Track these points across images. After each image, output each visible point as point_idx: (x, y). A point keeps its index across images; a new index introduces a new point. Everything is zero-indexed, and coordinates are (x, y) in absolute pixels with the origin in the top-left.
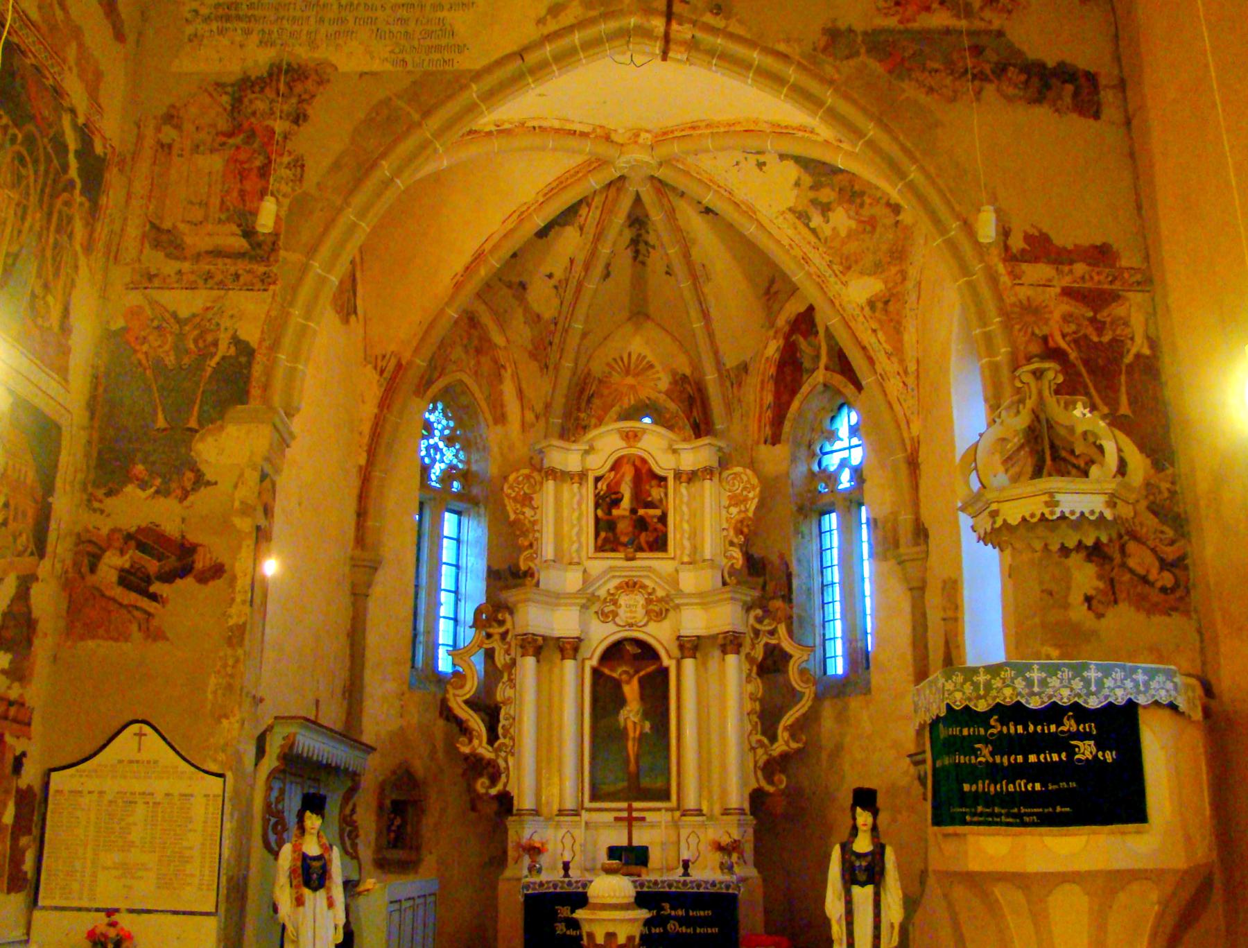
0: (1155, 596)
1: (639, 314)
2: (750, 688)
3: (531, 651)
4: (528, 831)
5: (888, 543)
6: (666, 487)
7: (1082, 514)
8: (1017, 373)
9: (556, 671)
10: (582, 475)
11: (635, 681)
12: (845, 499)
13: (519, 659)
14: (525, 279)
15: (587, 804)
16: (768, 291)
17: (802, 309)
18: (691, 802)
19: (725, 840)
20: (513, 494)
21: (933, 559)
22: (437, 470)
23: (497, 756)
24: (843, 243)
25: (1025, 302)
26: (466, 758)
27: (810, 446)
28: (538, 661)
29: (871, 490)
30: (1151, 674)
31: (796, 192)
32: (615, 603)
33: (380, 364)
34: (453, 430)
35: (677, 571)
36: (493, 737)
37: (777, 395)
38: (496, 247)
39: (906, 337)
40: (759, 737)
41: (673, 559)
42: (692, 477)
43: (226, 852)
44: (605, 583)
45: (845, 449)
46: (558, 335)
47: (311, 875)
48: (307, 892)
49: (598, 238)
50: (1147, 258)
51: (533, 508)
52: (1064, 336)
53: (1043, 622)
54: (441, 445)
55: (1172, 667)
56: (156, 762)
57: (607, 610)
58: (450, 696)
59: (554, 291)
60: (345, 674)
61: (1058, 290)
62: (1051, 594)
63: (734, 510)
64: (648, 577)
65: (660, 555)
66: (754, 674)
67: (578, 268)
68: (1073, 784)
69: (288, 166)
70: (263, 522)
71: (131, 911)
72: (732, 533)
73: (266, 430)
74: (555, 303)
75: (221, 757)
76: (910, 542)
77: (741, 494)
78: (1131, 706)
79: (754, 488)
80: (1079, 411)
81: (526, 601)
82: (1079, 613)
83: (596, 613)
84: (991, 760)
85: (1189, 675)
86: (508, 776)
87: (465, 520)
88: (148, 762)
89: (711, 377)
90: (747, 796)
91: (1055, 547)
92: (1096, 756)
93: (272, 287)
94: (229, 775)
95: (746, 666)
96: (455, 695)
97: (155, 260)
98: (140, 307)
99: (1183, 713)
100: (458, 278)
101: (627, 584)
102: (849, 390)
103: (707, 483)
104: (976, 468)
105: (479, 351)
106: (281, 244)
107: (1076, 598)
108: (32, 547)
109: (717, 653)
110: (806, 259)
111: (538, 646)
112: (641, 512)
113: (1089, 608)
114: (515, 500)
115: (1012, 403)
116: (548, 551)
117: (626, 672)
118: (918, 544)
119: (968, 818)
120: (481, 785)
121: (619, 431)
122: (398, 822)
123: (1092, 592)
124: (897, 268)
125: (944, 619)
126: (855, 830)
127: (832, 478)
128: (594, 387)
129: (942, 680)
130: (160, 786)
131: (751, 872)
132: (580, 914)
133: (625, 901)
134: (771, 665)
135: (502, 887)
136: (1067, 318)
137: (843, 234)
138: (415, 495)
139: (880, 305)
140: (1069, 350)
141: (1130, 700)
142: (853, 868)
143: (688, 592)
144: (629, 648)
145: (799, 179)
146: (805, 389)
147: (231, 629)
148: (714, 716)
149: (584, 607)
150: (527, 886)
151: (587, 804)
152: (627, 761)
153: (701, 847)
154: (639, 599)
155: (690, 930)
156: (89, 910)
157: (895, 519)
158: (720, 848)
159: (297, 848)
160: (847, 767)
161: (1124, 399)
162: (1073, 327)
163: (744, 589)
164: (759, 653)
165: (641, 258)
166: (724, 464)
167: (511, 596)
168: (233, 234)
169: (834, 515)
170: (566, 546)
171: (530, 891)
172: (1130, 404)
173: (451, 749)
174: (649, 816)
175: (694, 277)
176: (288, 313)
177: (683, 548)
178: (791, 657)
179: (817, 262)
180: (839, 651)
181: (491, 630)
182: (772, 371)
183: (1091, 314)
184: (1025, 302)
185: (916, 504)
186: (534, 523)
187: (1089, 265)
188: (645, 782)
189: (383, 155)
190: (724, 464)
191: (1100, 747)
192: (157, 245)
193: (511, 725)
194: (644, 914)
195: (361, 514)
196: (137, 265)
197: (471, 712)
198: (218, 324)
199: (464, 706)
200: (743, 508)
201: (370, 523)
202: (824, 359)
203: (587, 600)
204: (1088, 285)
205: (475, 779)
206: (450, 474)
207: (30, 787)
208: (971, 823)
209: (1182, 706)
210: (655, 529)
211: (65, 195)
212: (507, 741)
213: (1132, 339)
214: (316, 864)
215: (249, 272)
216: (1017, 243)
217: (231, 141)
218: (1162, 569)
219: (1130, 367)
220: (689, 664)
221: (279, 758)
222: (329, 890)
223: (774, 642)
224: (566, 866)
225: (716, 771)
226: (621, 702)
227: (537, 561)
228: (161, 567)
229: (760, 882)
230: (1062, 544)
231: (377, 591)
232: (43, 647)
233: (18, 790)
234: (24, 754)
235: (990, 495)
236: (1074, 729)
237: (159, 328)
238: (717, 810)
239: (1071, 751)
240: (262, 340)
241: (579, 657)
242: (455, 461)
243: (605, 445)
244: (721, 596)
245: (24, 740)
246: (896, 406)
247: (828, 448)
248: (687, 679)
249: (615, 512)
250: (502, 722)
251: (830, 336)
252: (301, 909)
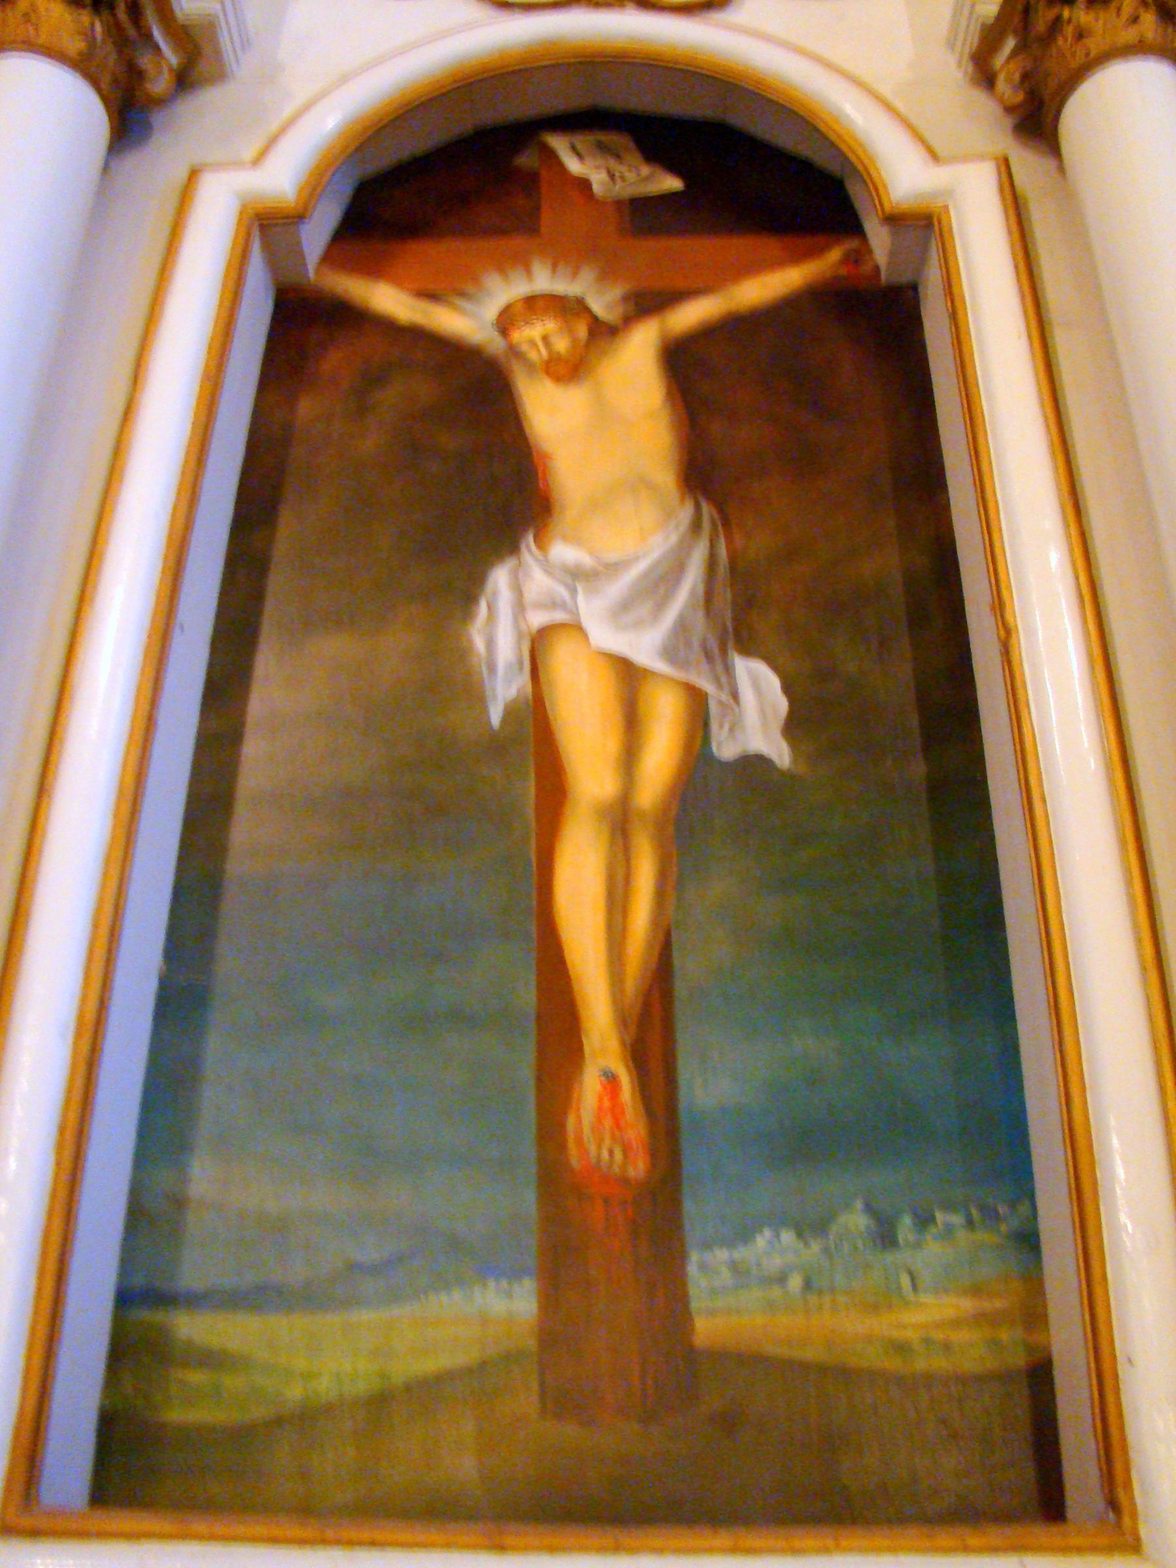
117: (534, 304)
188: (756, 1284)
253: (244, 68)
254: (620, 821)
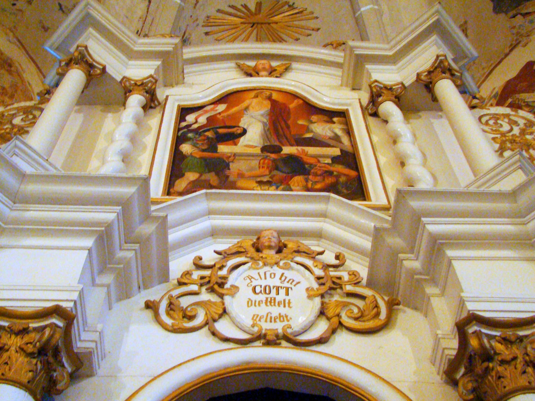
32: (217, 286)
83: (150, 306)
210: (330, 173)
249: (224, 149)
253: (102, 368)
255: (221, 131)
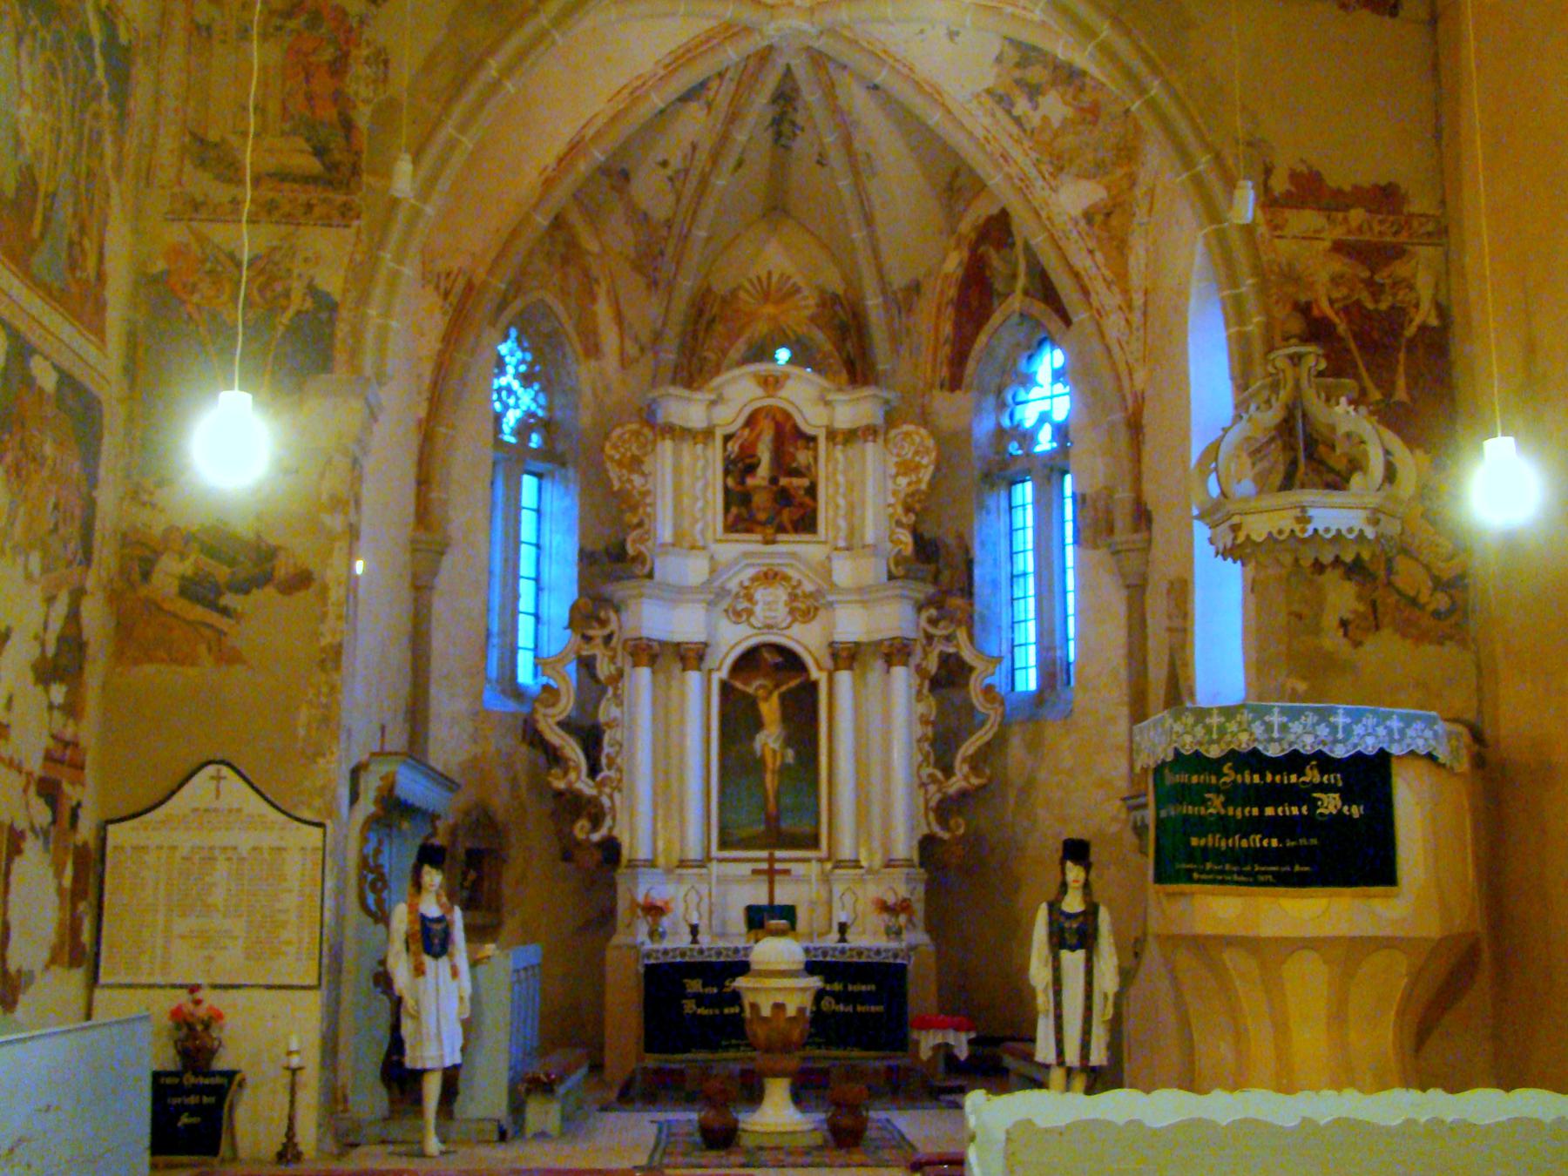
0: (1427, 622)
1: (777, 208)
2: (921, 708)
3: (645, 658)
4: (648, 887)
5: (1097, 525)
6: (816, 449)
7: (1339, 531)
8: (1271, 356)
9: (674, 684)
10: (708, 434)
11: (775, 695)
12: (1044, 466)
13: (627, 669)
14: (625, 166)
15: (715, 852)
16: (950, 188)
17: (995, 211)
18: (846, 851)
19: (890, 899)
20: (617, 457)
21: (1158, 550)
22: (511, 419)
23: (600, 793)
24: (1056, 135)
25: (1286, 269)
26: (559, 794)
27: (1000, 391)
28: (653, 673)
29: (1081, 452)
30: (1408, 721)
31: (995, 70)
32: (750, 598)
33: (443, 284)
34: (531, 365)
35: (829, 558)
36: (594, 770)
37: (957, 325)
38: (599, 134)
39: (1132, 261)
40: (931, 770)
41: (825, 542)
42: (851, 436)
43: (327, 919)
44: (735, 574)
45: (1045, 398)
46: (672, 242)
47: (430, 939)
48: (428, 960)
49: (733, 118)
50: (1443, 203)
51: (644, 475)
52: (1331, 302)
53: (1292, 650)
54: (516, 385)
55: (1433, 713)
56: (239, 810)
57: (739, 607)
58: (539, 716)
59: (666, 186)
60: (406, 690)
61: (1328, 244)
62: (1300, 617)
63: (903, 481)
64: (792, 566)
65: (805, 537)
66: (925, 691)
67: (703, 156)
68: (1314, 841)
69: (367, 62)
70: (353, 518)
71: (215, 987)
72: (900, 510)
73: (357, 405)
74: (671, 198)
75: (318, 802)
76: (1124, 526)
77: (912, 460)
78: (1383, 757)
79: (927, 452)
80: (1342, 407)
81: (641, 596)
82: (1333, 640)
83: (726, 611)
84: (1223, 811)
85: (1455, 720)
86: (614, 818)
87: (547, 485)
88: (230, 811)
89: (873, 302)
90: (915, 843)
91: (1306, 563)
92: (1340, 811)
93: (355, 223)
94: (329, 823)
95: (916, 681)
96: (545, 715)
97: (202, 184)
98: (187, 245)
99: (1444, 765)
100: (549, 172)
101: (766, 575)
102: (1055, 324)
103: (870, 446)
104: (1216, 469)
105: (565, 260)
106: (364, 164)
107: (1330, 621)
108: (80, 556)
109: (879, 665)
110: (1005, 157)
111: (649, 653)
112: (784, 481)
113: (1346, 634)
114: (620, 464)
115: (1263, 387)
116: (666, 533)
117: (761, 687)
118: (1136, 531)
119: (1195, 875)
120: (581, 829)
121: (755, 375)
122: (472, 875)
123: (1347, 615)
124: (1125, 169)
125: (1170, 630)
126: (1064, 887)
127: (1027, 438)
128: (715, 310)
129: (1169, 722)
130: (245, 841)
131: (919, 937)
132: (741, 982)
133: (794, 967)
134: (949, 677)
135: (611, 955)
136: (1336, 280)
137: (1056, 124)
138: (488, 454)
139: (1099, 218)
140: (1337, 320)
141: (1382, 750)
142: (1062, 930)
143: (845, 585)
144: (769, 657)
145: (1002, 53)
146: (996, 319)
147: (322, 650)
148: (875, 744)
149: (711, 604)
150: (648, 955)
151: (715, 852)
152: (766, 798)
153: (860, 907)
154: (780, 594)
155: (850, 1009)
156: (161, 987)
157: (1110, 497)
158: (884, 907)
159: (413, 908)
160: (1041, 812)
161: (1401, 383)
162: (1344, 291)
163: (915, 585)
164: (932, 665)
165: (783, 141)
166: (891, 419)
167: (618, 590)
168: (302, 151)
169: (1029, 486)
170: (686, 524)
171: (652, 961)
172: (1408, 387)
173: (539, 786)
174: (797, 868)
175: (855, 171)
176: (378, 258)
177: (838, 529)
178: (971, 669)
179: (1020, 158)
180: (1032, 660)
181: (591, 633)
182: (952, 292)
183: (1365, 274)
184: (1286, 269)
185: (1138, 478)
186: (646, 494)
187: (1370, 211)
188: (787, 824)
189: (490, 52)
190: (891, 419)
191: (1346, 800)
192: (202, 163)
193: (618, 753)
194: (815, 982)
195: (423, 482)
196: (176, 190)
197: (567, 737)
198: (289, 271)
199: (557, 729)
200: (914, 478)
201: (434, 495)
202: (1021, 282)
203: (714, 594)
204: (1367, 237)
205: (573, 822)
206: (523, 429)
207: (86, 844)
208: (1199, 881)
209: (1442, 757)
210: (801, 505)
211: (94, 106)
212: (612, 773)
213: (1417, 306)
214: (437, 927)
215: (324, 201)
216: (1280, 184)
217: (292, 24)
218: (1435, 588)
219: (1412, 345)
220: (844, 678)
221: (377, 801)
222: (451, 956)
223: (951, 650)
224: (694, 930)
225: (876, 809)
226: (758, 724)
227: (650, 543)
228: (233, 574)
229: (932, 949)
230: (1317, 560)
231: (442, 581)
232: (94, 673)
233: (76, 847)
234: (79, 805)
235: (1232, 507)
236: (1317, 780)
237: (211, 272)
238: (878, 861)
239: (1313, 805)
240: (346, 291)
241: (707, 664)
242: (533, 407)
243: (738, 393)
244: (888, 593)
245: (79, 788)
246: (1116, 349)
247: (1022, 396)
248: (843, 699)
249: (750, 482)
250: (607, 749)
251: (1028, 249)
252: (421, 979)
254: (773, 772)
255: (748, 461)
